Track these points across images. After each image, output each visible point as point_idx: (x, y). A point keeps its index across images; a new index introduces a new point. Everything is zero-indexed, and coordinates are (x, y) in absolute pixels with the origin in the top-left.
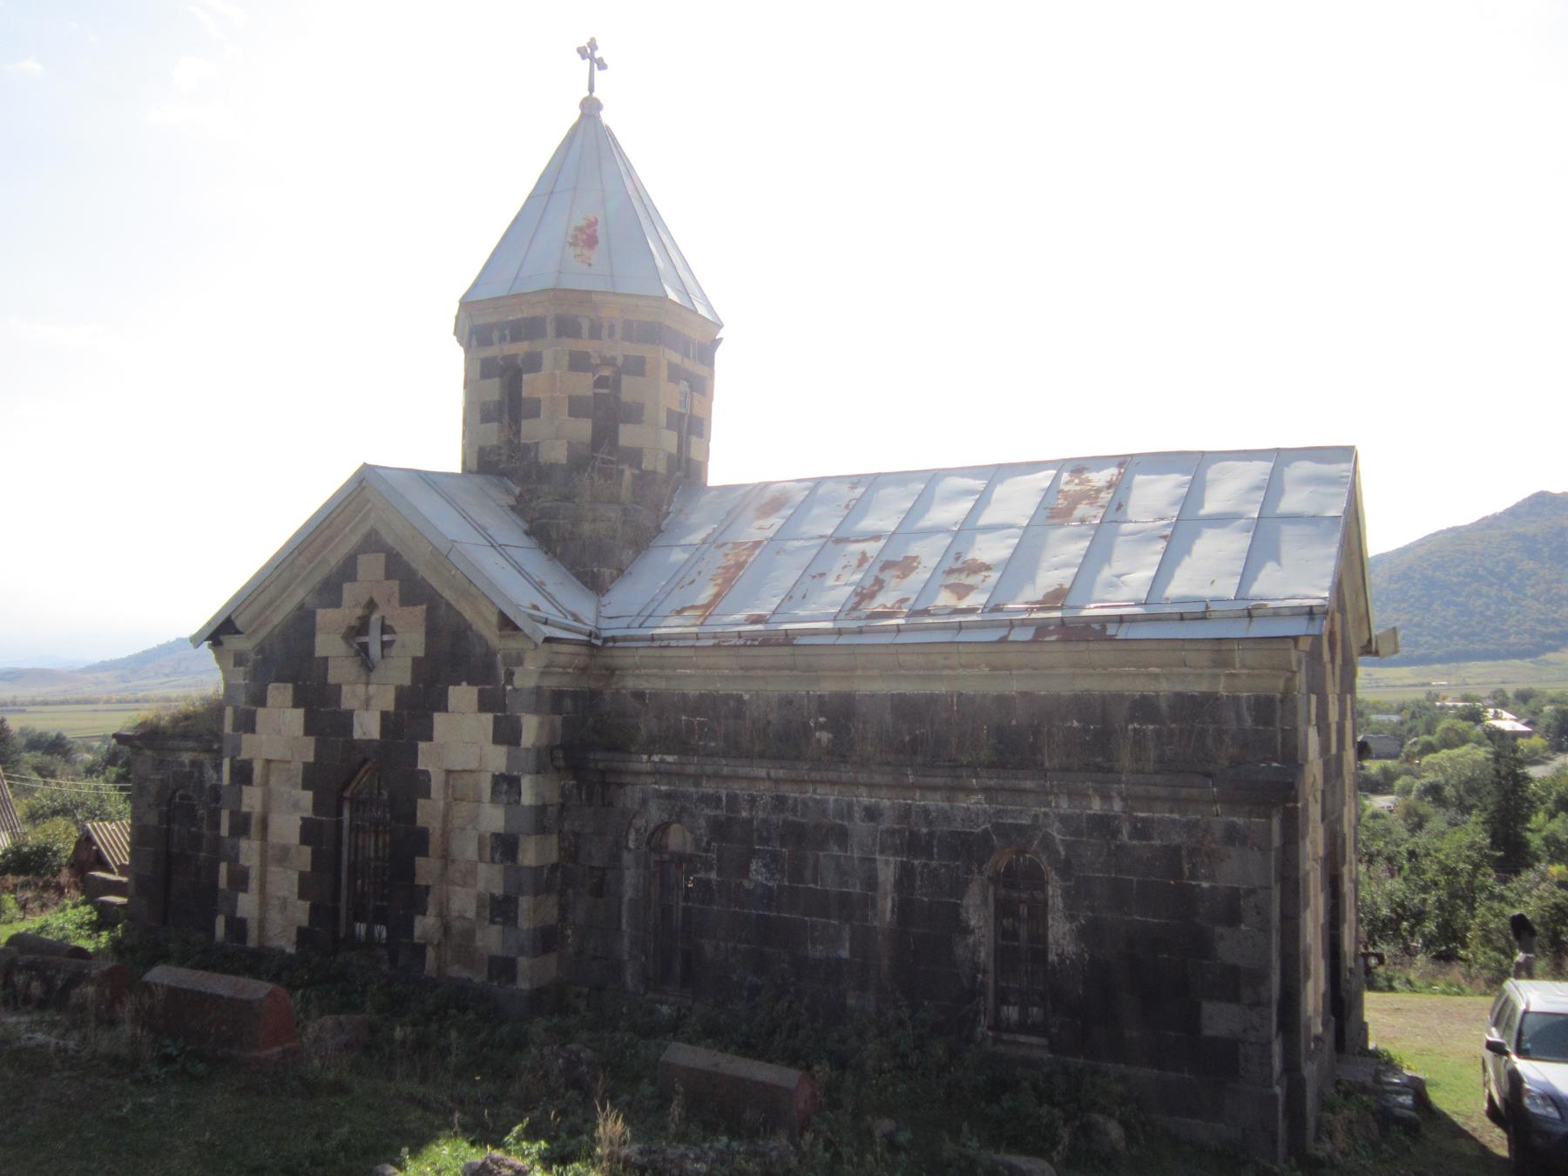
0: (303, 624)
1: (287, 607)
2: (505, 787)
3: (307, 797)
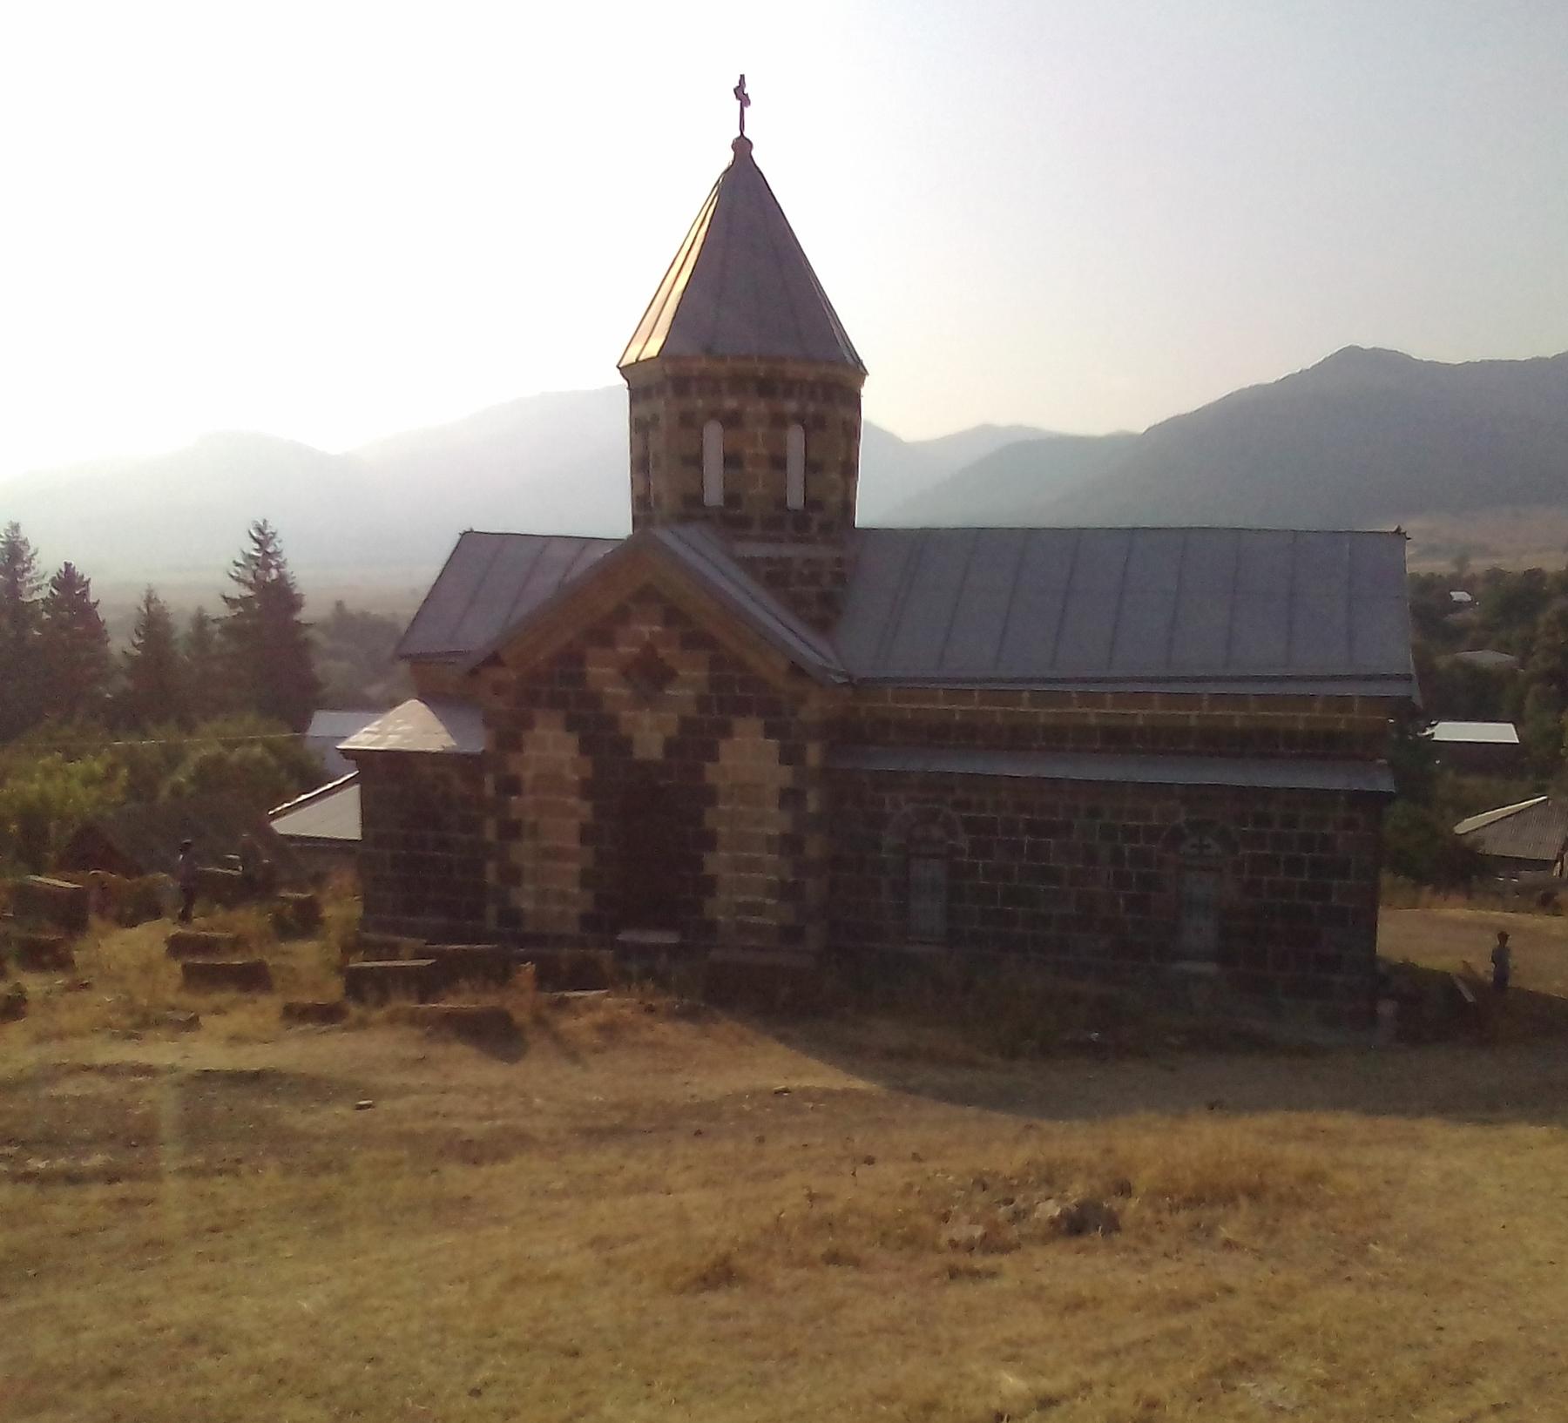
0: (572, 660)
3: (586, 809)
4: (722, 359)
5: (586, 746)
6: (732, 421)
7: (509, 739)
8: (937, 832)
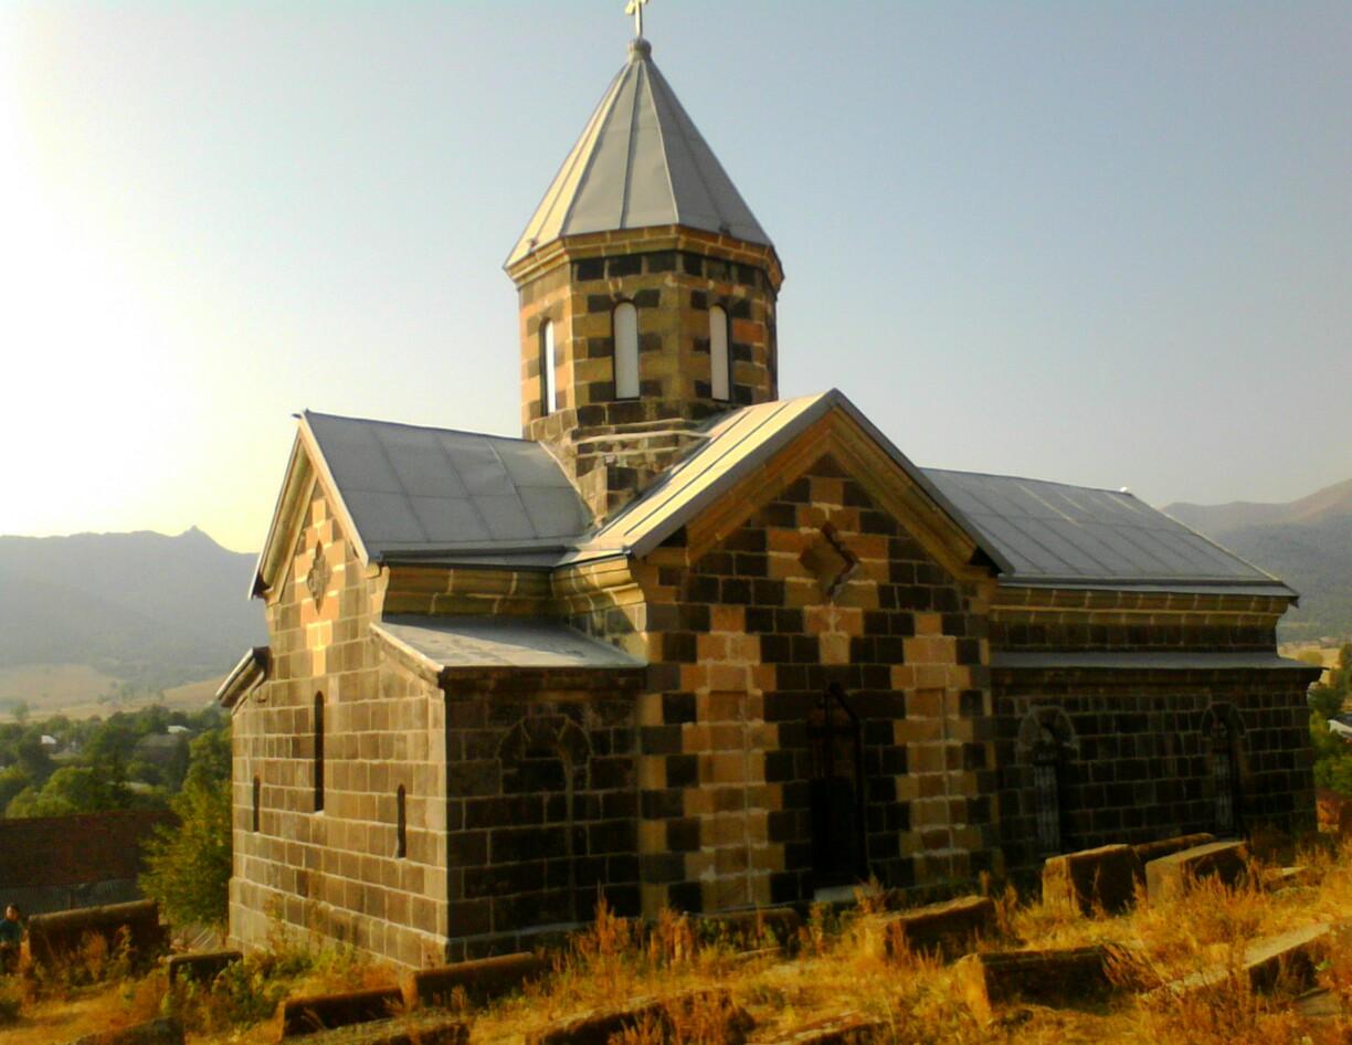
0: (752, 541)
1: (735, 523)
3: (771, 730)
4: (737, 242)
5: (770, 652)
6: (737, 311)
7: (679, 646)
8: (1048, 738)
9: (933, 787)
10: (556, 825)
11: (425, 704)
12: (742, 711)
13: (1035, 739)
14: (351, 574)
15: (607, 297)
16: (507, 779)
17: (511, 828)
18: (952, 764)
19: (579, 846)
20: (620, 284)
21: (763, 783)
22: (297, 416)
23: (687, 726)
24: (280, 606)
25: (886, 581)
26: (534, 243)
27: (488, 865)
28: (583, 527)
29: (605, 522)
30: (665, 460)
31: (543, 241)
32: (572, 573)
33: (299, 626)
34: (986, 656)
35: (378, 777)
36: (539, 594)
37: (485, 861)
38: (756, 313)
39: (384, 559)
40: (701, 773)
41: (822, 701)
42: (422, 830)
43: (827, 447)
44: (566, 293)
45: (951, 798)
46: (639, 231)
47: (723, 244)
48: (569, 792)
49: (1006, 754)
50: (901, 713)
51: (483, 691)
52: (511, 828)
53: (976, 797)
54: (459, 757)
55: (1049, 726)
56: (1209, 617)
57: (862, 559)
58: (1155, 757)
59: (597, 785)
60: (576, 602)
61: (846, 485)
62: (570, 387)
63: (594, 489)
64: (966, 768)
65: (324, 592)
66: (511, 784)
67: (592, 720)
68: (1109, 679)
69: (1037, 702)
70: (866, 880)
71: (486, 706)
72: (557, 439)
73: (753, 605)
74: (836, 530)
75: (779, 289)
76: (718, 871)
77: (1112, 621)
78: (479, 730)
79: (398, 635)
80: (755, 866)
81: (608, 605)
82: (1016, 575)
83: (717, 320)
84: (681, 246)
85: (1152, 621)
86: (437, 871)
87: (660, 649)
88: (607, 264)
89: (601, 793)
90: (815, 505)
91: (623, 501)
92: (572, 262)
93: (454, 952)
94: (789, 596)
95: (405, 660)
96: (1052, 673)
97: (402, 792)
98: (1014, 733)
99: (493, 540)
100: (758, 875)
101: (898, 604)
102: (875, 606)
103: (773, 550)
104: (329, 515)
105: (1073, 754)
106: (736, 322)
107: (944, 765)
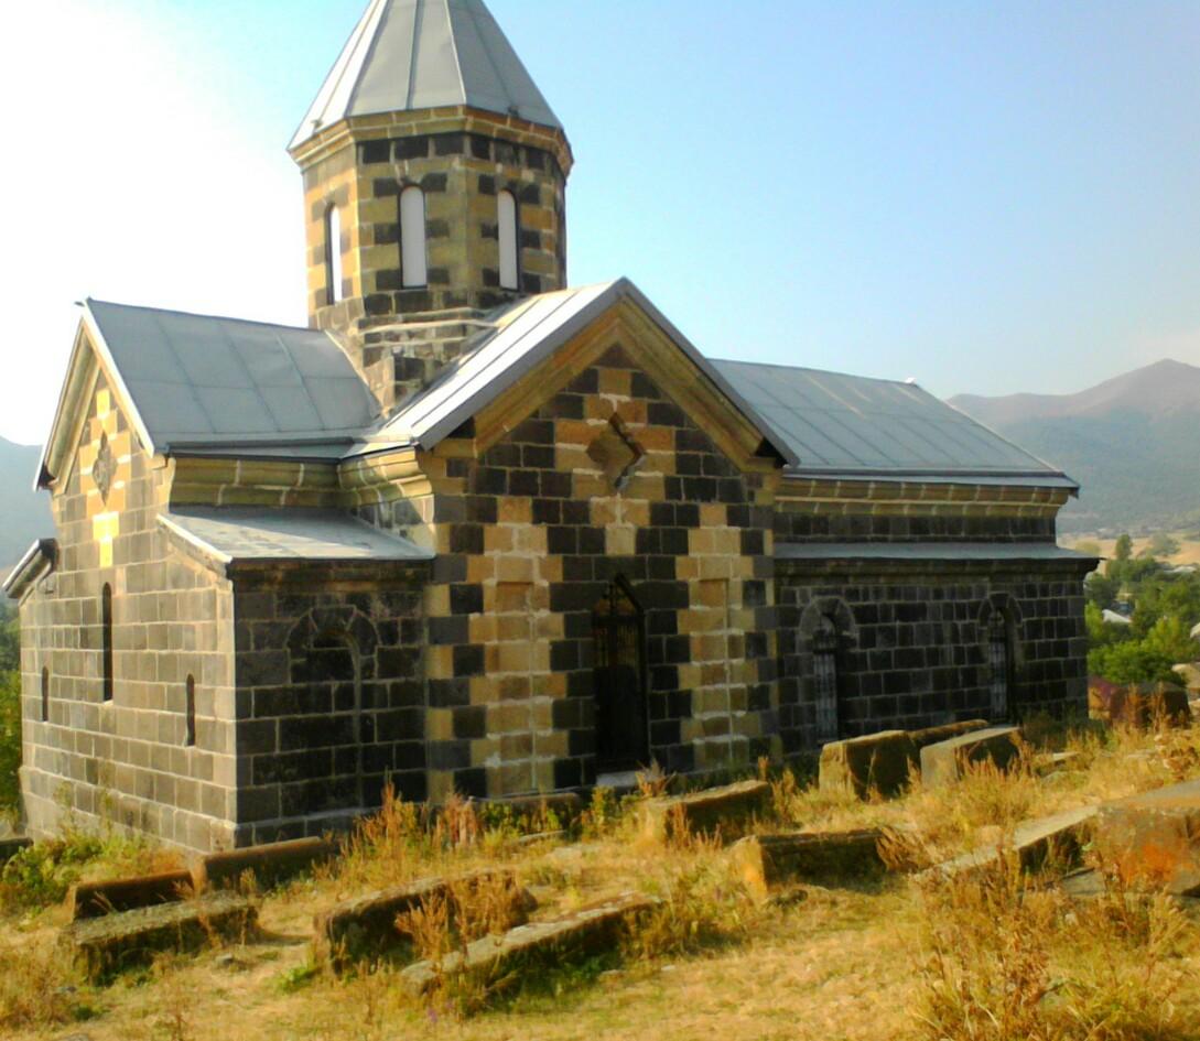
0: (539, 432)
1: (522, 415)
2: (753, 592)
3: (557, 621)
4: (526, 124)
5: (557, 543)
6: (526, 196)
7: (467, 539)
8: (828, 627)
9: (714, 675)
10: (344, 713)
11: (213, 595)
12: (528, 601)
13: (816, 628)
14: (137, 464)
15: (393, 181)
16: (296, 669)
17: (299, 716)
18: (734, 654)
19: (367, 734)
20: (407, 168)
21: (548, 672)
22: (79, 304)
23: (473, 617)
24: (67, 498)
25: (673, 473)
26: (318, 124)
27: (277, 752)
28: (371, 419)
29: (392, 413)
30: (452, 349)
31: (327, 122)
32: (359, 465)
33: (84, 517)
34: (769, 548)
35: (166, 667)
36: (325, 485)
37: (273, 748)
38: (544, 197)
39: (171, 451)
40: (487, 661)
41: (608, 591)
42: (211, 718)
43: (616, 337)
44: (352, 176)
45: (733, 686)
46: (425, 112)
47: (512, 125)
48: (357, 682)
49: (787, 643)
50: (685, 604)
51: (271, 581)
52: (299, 716)
53: (756, 685)
54: (248, 648)
55: (830, 616)
56: (990, 508)
57: (649, 451)
58: (933, 646)
59: (384, 674)
60: (363, 493)
61: (634, 375)
62: (357, 274)
63: (380, 378)
64: (748, 657)
65: (109, 484)
66: (299, 674)
67: (379, 611)
68: (892, 570)
69: (820, 592)
70: (648, 765)
71: (275, 596)
72: (344, 328)
73: (540, 497)
74: (622, 422)
75: (568, 173)
76: (504, 757)
77: (896, 512)
78: (267, 621)
79: (186, 527)
80: (539, 753)
81: (393, 497)
82: (801, 467)
83: (505, 205)
84: (468, 128)
85: (934, 512)
86: (226, 758)
87: (447, 540)
88: (393, 148)
89: (388, 682)
90: (602, 395)
91: (411, 392)
92: (358, 144)
93: (242, 837)
94: (576, 487)
95: (193, 552)
96: (834, 563)
97: (191, 682)
98: (795, 622)
99: (279, 431)
100: (542, 761)
101: (684, 497)
102: (660, 496)
103: (561, 441)
104: (113, 405)
105: (852, 642)
106: (525, 208)
107: (726, 654)
